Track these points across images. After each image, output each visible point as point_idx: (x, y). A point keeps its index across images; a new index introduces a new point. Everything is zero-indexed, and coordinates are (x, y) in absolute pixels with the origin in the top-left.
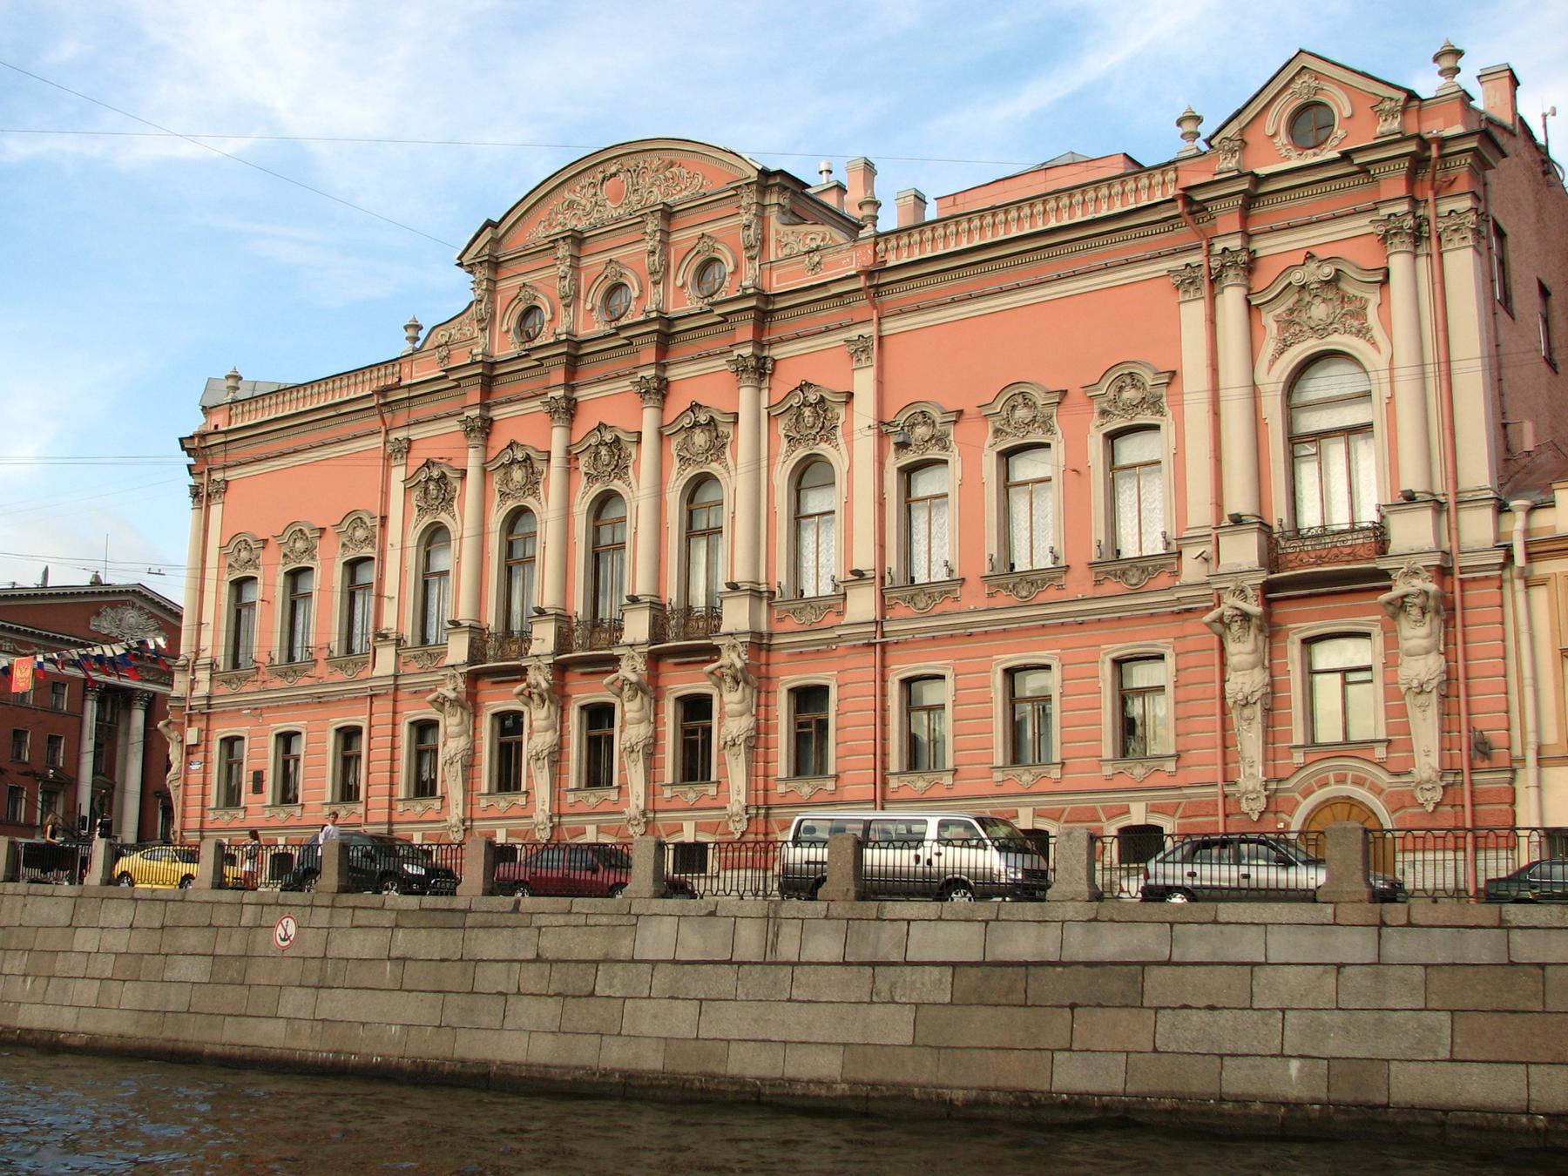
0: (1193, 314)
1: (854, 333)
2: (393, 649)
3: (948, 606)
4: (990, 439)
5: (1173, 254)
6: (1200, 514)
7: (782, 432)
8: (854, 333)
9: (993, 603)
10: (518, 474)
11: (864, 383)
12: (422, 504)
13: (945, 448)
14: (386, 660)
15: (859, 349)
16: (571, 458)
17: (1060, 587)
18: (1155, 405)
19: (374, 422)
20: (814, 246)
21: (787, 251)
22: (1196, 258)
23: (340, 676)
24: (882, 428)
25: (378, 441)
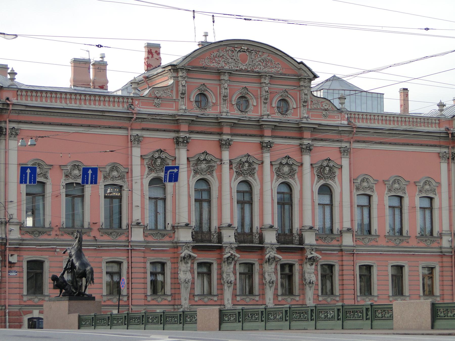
0: (444, 166)
1: (344, 145)
2: (142, 230)
3: (373, 243)
4: (386, 192)
5: (440, 146)
6: (446, 227)
7: (316, 173)
8: (344, 145)
9: (390, 244)
10: (203, 166)
11: (345, 162)
12: (151, 167)
13: (373, 192)
14: (137, 236)
15: (344, 152)
16: (231, 163)
17: (408, 242)
18: (434, 191)
19: (125, 123)
20: (326, 108)
21: (315, 106)
22: (446, 150)
23: (106, 238)
24: (352, 181)
25: (122, 132)
